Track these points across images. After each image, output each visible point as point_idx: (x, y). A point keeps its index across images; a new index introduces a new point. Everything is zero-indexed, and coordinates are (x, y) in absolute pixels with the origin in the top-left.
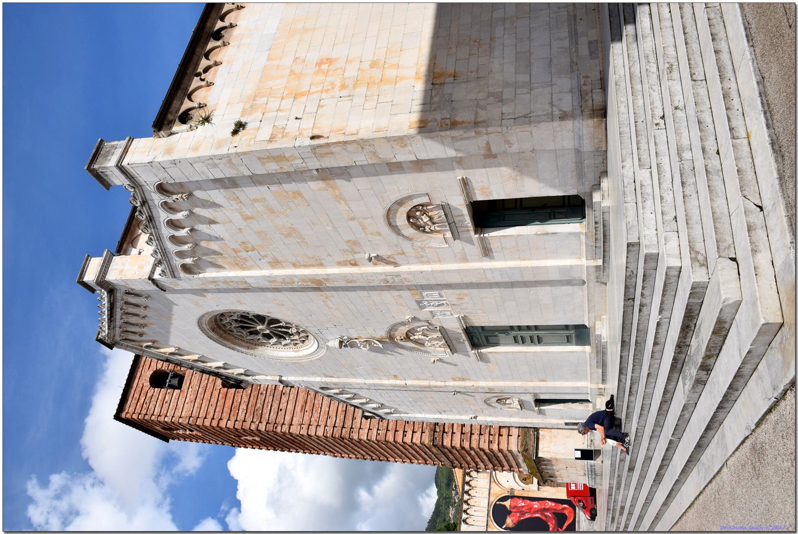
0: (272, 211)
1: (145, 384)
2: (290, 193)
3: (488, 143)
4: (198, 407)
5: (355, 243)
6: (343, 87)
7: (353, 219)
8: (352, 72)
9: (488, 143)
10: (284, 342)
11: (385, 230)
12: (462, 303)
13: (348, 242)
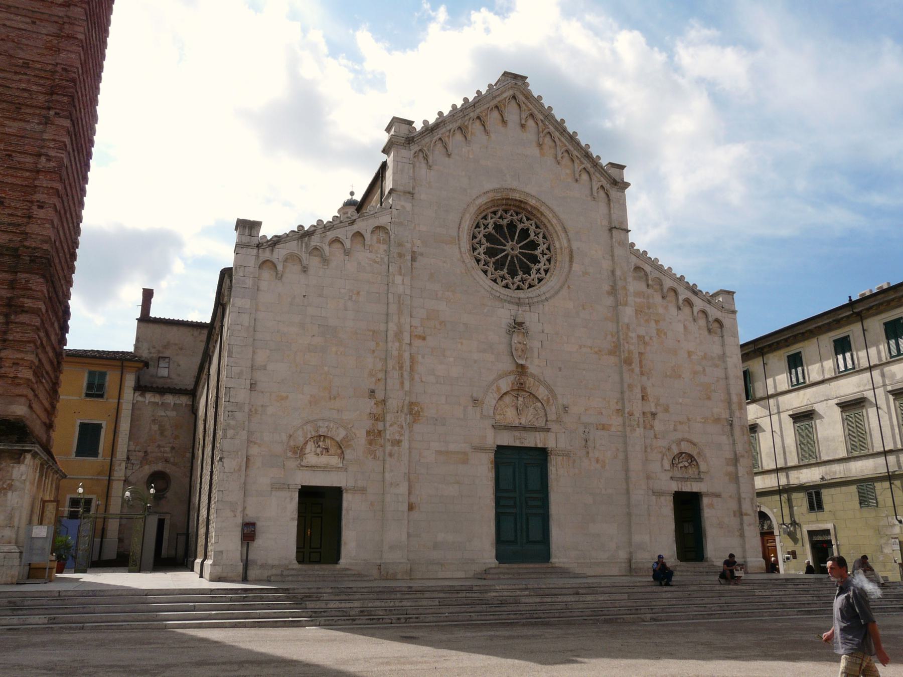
3: (749, 515)
5: (666, 410)
7: (689, 420)
9: (749, 515)
11: (679, 435)
12: (590, 460)
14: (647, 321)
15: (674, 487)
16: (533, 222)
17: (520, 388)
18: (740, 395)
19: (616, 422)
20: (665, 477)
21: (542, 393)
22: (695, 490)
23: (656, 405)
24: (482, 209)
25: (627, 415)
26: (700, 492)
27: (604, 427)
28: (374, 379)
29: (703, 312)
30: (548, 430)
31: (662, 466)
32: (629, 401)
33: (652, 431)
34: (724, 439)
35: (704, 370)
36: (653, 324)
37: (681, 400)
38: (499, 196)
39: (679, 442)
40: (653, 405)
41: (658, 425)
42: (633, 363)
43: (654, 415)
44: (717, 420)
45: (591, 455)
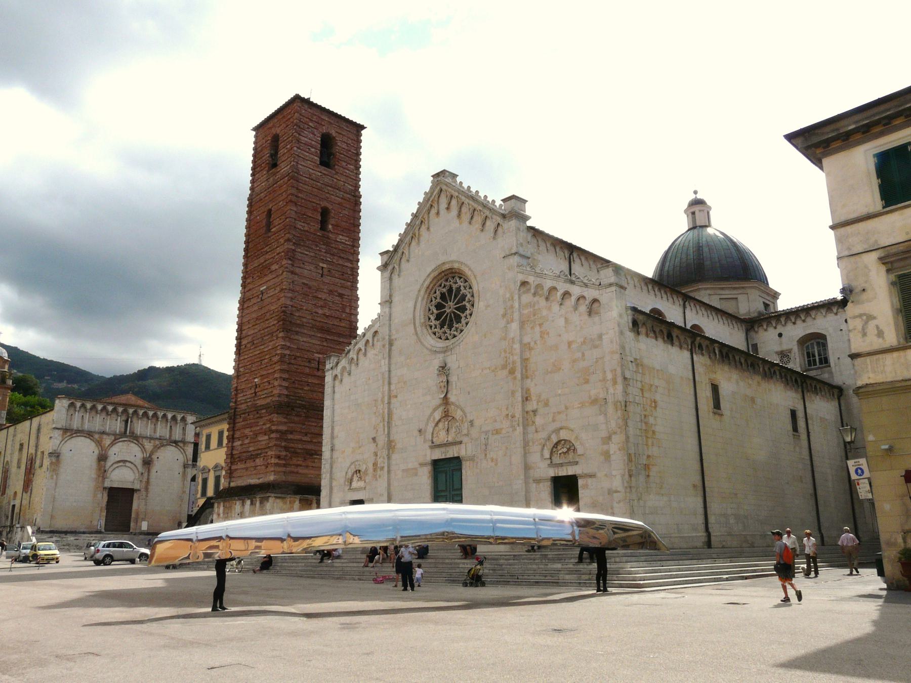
0: (574, 361)
1: (324, 127)
2: (588, 377)
4: (305, 181)
5: (546, 404)
6: (645, 416)
7: (567, 408)
8: (651, 420)
10: (432, 318)
11: (557, 425)
12: (487, 460)
13: (548, 400)
14: (532, 328)
15: (552, 473)
16: (462, 279)
17: (446, 415)
18: (615, 370)
19: (505, 424)
20: (543, 465)
21: (458, 414)
22: (570, 473)
23: (538, 402)
24: (431, 287)
25: (510, 418)
26: (575, 475)
27: (497, 432)
28: (375, 431)
29: (579, 299)
30: (461, 443)
31: (542, 455)
32: (512, 406)
33: (534, 427)
34: (601, 418)
35: (583, 355)
36: (537, 329)
37: (560, 392)
38: (436, 273)
39: (557, 431)
40: (535, 403)
41: (539, 420)
42: (515, 371)
43: (535, 412)
44: (594, 402)
45: (488, 455)
